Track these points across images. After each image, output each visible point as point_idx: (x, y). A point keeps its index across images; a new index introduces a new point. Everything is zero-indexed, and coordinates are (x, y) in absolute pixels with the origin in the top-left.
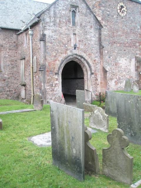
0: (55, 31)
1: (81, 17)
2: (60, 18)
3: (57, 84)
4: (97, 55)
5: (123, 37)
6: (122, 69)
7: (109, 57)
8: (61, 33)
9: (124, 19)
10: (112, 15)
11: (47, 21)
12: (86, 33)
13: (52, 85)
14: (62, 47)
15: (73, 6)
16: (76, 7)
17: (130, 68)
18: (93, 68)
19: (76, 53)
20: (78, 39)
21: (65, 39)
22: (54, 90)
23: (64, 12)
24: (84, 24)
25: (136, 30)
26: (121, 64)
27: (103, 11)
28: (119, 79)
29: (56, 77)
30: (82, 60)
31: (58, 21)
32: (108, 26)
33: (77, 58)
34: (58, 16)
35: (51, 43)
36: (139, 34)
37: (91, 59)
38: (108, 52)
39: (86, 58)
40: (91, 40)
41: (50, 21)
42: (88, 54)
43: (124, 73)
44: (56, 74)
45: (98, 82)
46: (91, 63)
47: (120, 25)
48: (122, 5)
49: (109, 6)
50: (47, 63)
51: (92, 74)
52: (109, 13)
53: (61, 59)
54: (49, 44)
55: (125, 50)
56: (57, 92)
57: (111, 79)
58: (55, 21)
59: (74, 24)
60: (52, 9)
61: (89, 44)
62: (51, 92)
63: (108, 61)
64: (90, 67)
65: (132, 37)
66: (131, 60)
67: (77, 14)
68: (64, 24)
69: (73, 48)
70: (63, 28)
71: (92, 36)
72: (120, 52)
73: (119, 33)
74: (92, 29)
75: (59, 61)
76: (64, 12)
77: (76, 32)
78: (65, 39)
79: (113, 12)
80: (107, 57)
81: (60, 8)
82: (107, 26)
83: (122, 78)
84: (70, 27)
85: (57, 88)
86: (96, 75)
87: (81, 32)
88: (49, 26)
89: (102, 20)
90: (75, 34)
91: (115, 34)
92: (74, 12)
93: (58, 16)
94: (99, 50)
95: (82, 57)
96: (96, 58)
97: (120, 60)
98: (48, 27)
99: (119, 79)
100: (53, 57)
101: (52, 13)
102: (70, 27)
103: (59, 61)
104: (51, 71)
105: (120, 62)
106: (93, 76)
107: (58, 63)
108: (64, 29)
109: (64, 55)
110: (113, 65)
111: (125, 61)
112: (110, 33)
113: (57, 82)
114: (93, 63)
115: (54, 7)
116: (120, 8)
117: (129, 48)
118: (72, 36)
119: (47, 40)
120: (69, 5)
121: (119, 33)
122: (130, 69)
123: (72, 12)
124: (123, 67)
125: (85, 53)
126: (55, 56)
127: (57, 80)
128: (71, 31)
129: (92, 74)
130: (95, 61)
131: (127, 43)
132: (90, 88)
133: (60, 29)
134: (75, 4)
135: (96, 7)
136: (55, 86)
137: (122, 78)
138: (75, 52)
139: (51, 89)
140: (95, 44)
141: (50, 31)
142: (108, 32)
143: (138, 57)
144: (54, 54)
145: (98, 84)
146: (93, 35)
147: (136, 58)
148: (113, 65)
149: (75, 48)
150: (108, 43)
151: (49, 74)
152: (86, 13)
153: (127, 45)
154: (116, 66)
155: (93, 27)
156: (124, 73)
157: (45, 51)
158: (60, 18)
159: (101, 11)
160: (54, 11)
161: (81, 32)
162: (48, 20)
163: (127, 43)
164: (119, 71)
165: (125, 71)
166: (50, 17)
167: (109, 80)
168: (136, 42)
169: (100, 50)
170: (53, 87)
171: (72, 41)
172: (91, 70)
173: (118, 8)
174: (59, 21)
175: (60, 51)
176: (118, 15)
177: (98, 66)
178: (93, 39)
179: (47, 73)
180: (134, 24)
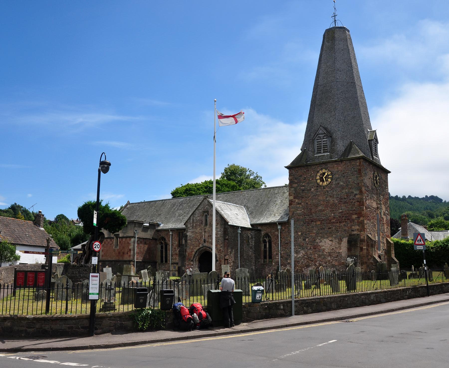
0: (193, 232)
6: (325, 253)
10: (309, 188)
15: (204, 212)
17: (341, 251)
27: (295, 189)
31: (195, 225)
32: (302, 203)
34: (195, 221)
36: (358, 201)
43: (329, 258)
44: (192, 261)
49: (304, 179)
52: (303, 188)
53: (195, 250)
58: (193, 225)
60: (192, 218)
65: (343, 208)
66: (341, 240)
72: (321, 231)
73: (320, 208)
76: (198, 218)
80: (300, 240)
82: (301, 204)
86: (221, 261)
89: (294, 198)
92: (206, 216)
93: (195, 221)
97: (321, 242)
101: (192, 220)
105: (320, 244)
107: (194, 253)
108: (198, 230)
109: (198, 248)
111: (330, 243)
112: (305, 211)
117: (338, 225)
121: (320, 208)
122: (339, 252)
124: (327, 250)
126: (192, 249)
128: (203, 230)
130: (220, 250)
148: (310, 248)
149: (205, 242)
150: (302, 223)
153: (334, 221)
156: (329, 258)
159: (293, 189)
162: (189, 226)
163: (334, 218)
164: (319, 256)
171: (203, 237)
176: (317, 187)
178: (219, 233)
180: (347, 190)
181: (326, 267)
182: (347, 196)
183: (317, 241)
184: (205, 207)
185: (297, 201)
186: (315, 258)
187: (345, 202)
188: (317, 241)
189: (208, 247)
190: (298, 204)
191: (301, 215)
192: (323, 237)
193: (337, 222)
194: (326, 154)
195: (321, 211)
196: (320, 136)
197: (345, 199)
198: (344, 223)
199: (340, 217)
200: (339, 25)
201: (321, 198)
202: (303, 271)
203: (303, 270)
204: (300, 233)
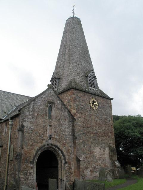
0: (33, 123)
1: (56, 111)
2: (38, 112)
3: (31, 173)
4: (71, 145)
5: (96, 128)
7: (84, 146)
8: (38, 125)
9: (96, 112)
10: (85, 108)
11: (27, 114)
12: (60, 125)
13: (27, 174)
14: (39, 137)
15: (50, 102)
16: (53, 103)
17: (105, 157)
18: (67, 157)
19: (51, 142)
20: (53, 130)
21: (42, 130)
22: (27, 179)
23: (41, 107)
24: (59, 117)
25: (108, 121)
26: (96, 153)
27: (77, 105)
28: (95, 168)
29: (31, 166)
30: (57, 149)
31: (36, 114)
33: (52, 148)
34: (37, 110)
35: (29, 133)
37: (65, 149)
38: (82, 142)
39: (60, 148)
40: (65, 131)
41: (29, 114)
42: (62, 144)
43: (99, 162)
44: (31, 162)
45: (72, 171)
46: (65, 152)
47: (92, 117)
48: (94, 100)
49: (83, 101)
50: (23, 152)
51: (66, 163)
53: (36, 148)
54: (27, 134)
55: (98, 140)
56: (31, 181)
57: (87, 168)
58: (33, 115)
59: (50, 117)
60: (32, 104)
61: (63, 135)
62: (25, 181)
63: (82, 150)
64: (64, 156)
66: (104, 149)
67: (53, 109)
68: (42, 117)
69: (49, 138)
70: (41, 121)
71: (67, 128)
72: (94, 141)
73: (92, 124)
74: (66, 121)
75: (35, 150)
76: (41, 107)
77: (52, 124)
78: (42, 130)
79: (87, 106)
81: (38, 104)
82: (81, 118)
83: (97, 167)
84: (46, 119)
85: (31, 177)
86: (70, 164)
87: (56, 124)
88: (28, 118)
89: (77, 112)
90: (50, 126)
91: (89, 125)
92: (50, 107)
93: (37, 110)
94: (72, 141)
95: (56, 146)
96: (70, 148)
98: (27, 120)
99: (95, 168)
100: (30, 146)
101: (31, 107)
102: (46, 119)
103: (35, 150)
104: (26, 160)
106: (67, 165)
107: (34, 152)
109: (40, 145)
110: (88, 154)
111: (99, 150)
113: (31, 171)
114: (67, 153)
115: (33, 103)
116: (93, 102)
118: (48, 127)
119: (25, 130)
120: (47, 102)
121: (92, 124)
122: (104, 158)
123: (49, 107)
125: (59, 143)
126: (31, 145)
127: (32, 168)
128: (48, 124)
129: (66, 163)
130: (68, 150)
131: (101, 133)
132: (64, 177)
133: (37, 121)
134: (52, 101)
135: (71, 101)
136: (30, 175)
137: (97, 167)
138: (51, 141)
139: (25, 178)
140: (69, 135)
141: (29, 123)
142: (82, 123)
143: (111, 146)
144: (31, 144)
145: (72, 173)
146: (67, 127)
147: (109, 146)
148: (88, 154)
149: (50, 138)
150: (82, 133)
151: (25, 162)
152: (61, 108)
154: (90, 155)
155: (67, 119)
157: (22, 141)
158: (38, 112)
159: (76, 105)
160: (33, 106)
161: (56, 124)
162: (27, 113)
163: (101, 133)
164: (94, 160)
165: (99, 160)
166: (29, 111)
167: (84, 169)
168: (109, 132)
169: (73, 141)
170: (27, 176)
171: (48, 131)
172: (65, 159)
173: (91, 103)
174: (37, 114)
175: (36, 141)
176: (90, 109)
177: (71, 155)
178: (67, 130)
179: (23, 161)
181: (98, 168)
182: (106, 120)
183: (92, 148)
184: (49, 97)
185: (78, 115)
186: (91, 162)
187: (105, 124)
188: (92, 148)
189: (54, 145)
190: (79, 118)
191: (81, 127)
192: (95, 146)
193: (102, 136)
194: (95, 89)
195: (93, 126)
196: (91, 76)
197: (105, 122)
198: (106, 138)
199: (103, 133)
200: (75, 16)
201: (92, 117)
202: (84, 173)
203: (84, 171)
204: (81, 141)
